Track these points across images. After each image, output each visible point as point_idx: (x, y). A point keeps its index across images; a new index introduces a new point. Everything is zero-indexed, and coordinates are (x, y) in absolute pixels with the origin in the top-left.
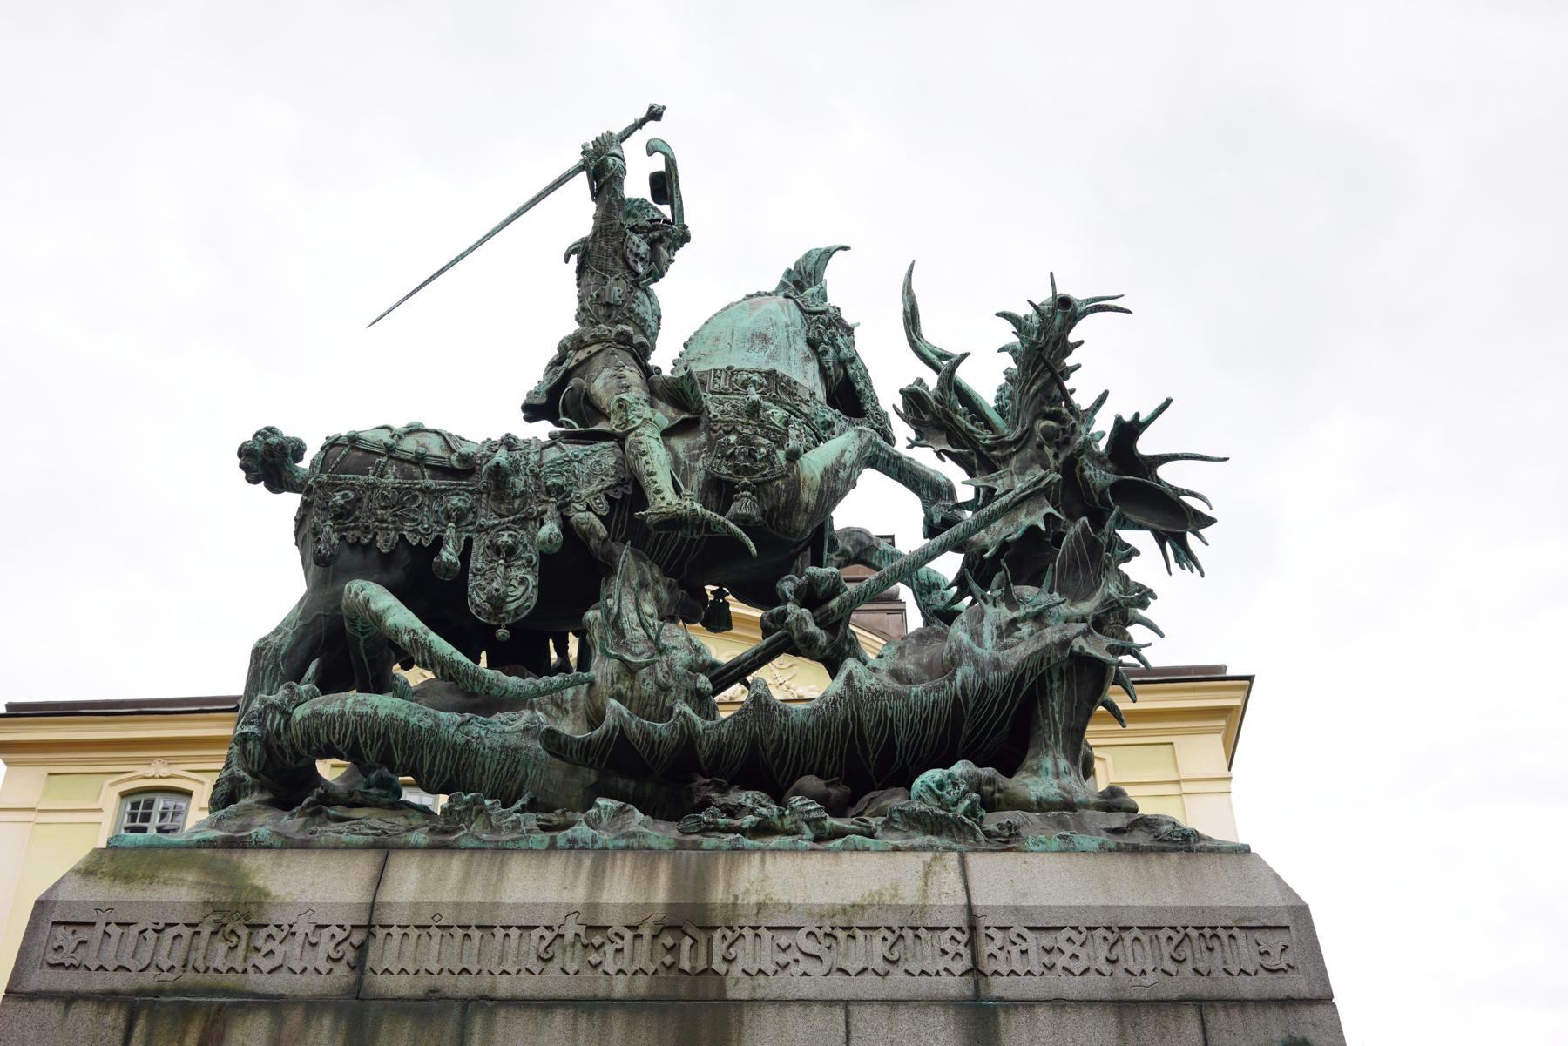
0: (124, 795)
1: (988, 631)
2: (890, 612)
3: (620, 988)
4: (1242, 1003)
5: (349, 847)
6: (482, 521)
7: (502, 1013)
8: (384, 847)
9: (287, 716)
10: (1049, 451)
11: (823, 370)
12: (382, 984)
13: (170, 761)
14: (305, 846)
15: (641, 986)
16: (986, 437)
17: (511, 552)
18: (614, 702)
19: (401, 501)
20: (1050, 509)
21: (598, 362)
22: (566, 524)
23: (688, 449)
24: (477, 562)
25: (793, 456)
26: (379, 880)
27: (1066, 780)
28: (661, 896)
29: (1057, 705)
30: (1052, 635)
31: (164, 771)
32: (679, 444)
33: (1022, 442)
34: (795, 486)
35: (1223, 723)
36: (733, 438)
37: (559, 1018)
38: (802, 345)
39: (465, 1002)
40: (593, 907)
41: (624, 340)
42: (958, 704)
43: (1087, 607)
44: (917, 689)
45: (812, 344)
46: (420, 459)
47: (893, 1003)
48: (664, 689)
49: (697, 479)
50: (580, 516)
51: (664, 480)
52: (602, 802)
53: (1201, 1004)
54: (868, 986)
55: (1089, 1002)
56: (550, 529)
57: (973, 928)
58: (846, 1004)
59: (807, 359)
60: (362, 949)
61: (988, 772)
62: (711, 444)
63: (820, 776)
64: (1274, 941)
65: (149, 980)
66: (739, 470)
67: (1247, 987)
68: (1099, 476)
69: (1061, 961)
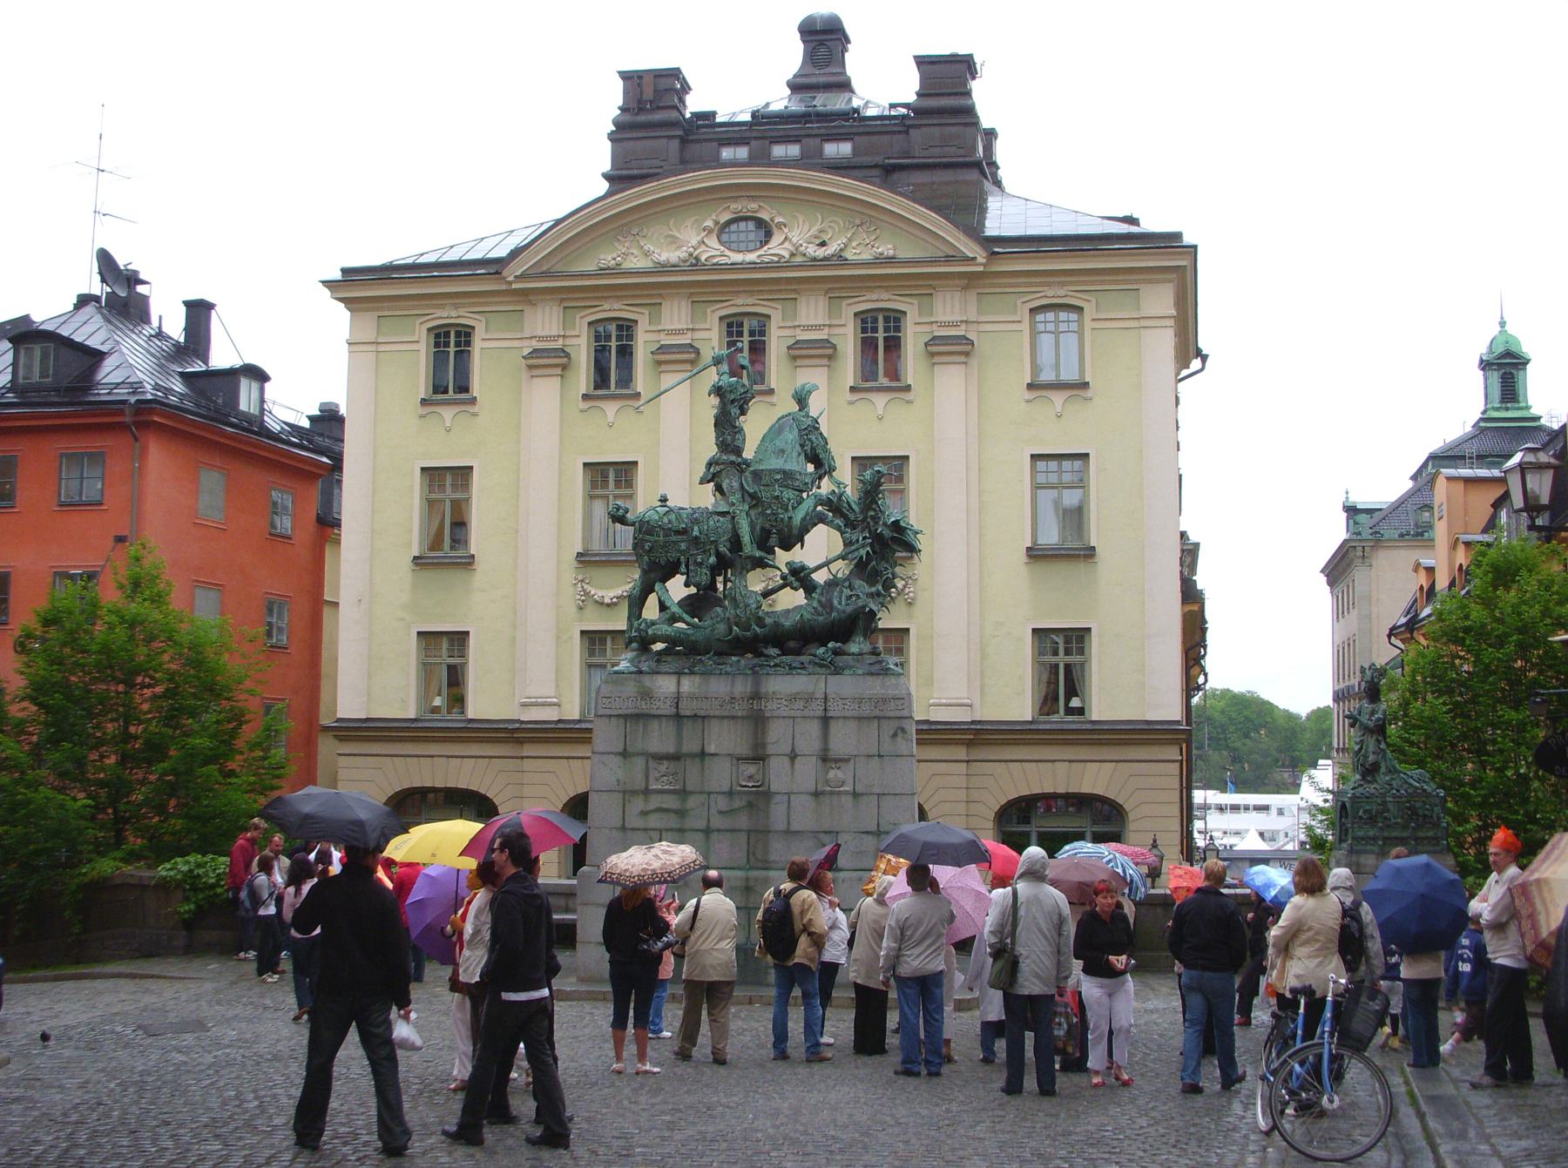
0: (429, 330)
1: (843, 598)
2: (965, 125)
3: (740, 714)
4: (889, 718)
5: (669, 673)
6: (691, 552)
7: (713, 720)
8: (679, 674)
9: (647, 633)
10: (871, 524)
11: (806, 455)
12: (682, 713)
13: (456, 307)
14: (658, 673)
15: (745, 713)
16: (852, 517)
17: (700, 564)
18: (735, 628)
19: (665, 546)
20: (869, 549)
21: (724, 473)
22: (718, 555)
23: (756, 514)
24: (691, 568)
25: (790, 518)
26: (679, 683)
27: (862, 645)
28: (749, 690)
29: (861, 623)
30: (860, 603)
31: (454, 314)
32: (753, 513)
33: (864, 520)
34: (790, 529)
35: (1175, 276)
36: (768, 512)
37: (725, 721)
38: (798, 448)
39: (703, 717)
40: (732, 693)
41: (732, 463)
42: (833, 623)
43: (873, 589)
44: (821, 618)
45: (802, 446)
46: (670, 529)
47: (804, 717)
48: (748, 619)
49: (758, 528)
50: (722, 549)
51: (746, 538)
52: (734, 658)
53: (879, 718)
54: (798, 713)
55: (853, 718)
56: (712, 560)
57: (826, 698)
58: (793, 717)
59: (799, 454)
60: (677, 703)
61: (839, 644)
62: (763, 513)
63: (794, 639)
64: (897, 702)
65: (627, 712)
66: (772, 526)
67: (892, 714)
68: (887, 533)
69: (846, 707)
